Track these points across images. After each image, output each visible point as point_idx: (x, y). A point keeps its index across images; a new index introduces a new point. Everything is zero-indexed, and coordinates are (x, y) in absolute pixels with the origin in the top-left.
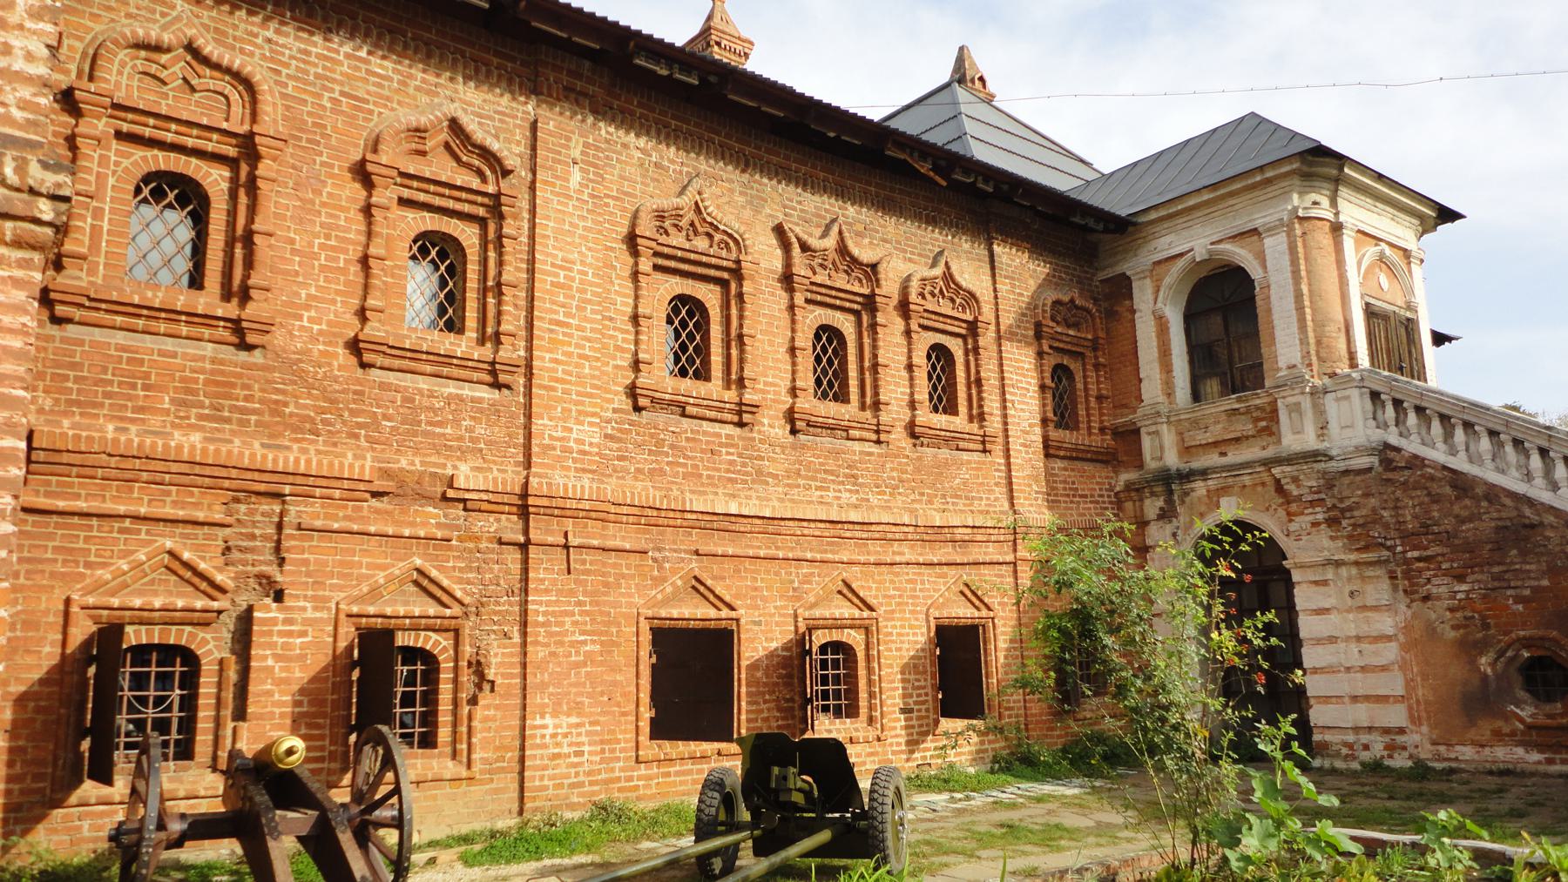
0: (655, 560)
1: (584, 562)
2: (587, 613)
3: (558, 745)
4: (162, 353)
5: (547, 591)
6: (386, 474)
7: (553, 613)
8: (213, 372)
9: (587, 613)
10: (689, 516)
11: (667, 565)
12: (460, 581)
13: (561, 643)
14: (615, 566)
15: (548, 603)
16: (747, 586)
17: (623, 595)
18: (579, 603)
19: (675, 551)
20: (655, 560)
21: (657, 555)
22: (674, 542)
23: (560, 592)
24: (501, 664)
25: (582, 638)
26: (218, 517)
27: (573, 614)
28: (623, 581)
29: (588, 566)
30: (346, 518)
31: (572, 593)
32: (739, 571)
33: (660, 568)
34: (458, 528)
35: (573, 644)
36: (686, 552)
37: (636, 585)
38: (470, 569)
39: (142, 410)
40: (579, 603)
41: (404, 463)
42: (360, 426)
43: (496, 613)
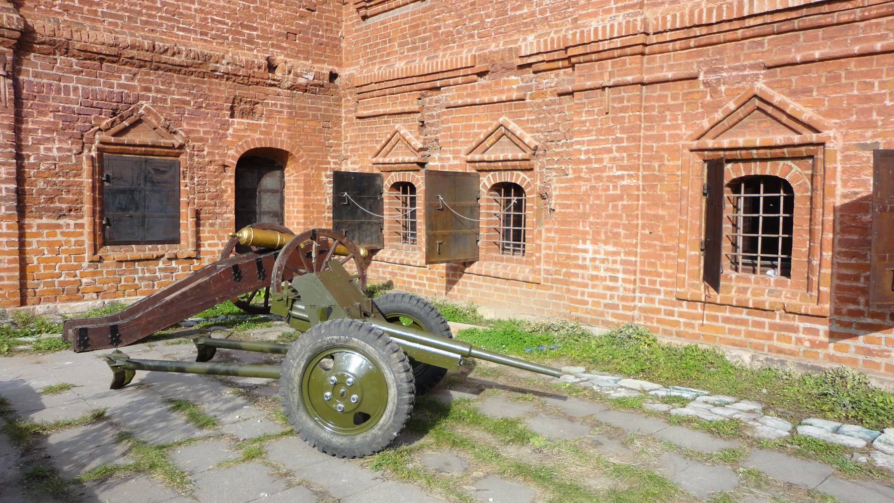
0: (706, 84)
1: (621, 100)
2: (625, 149)
3: (596, 268)
4: (396, 18)
5: (588, 132)
6: (484, 58)
7: (594, 152)
8: (413, 20)
9: (625, 149)
10: (752, 22)
11: (723, 88)
12: (532, 130)
13: (599, 179)
14: (661, 98)
15: (590, 142)
16: (850, 97)
17: (667, 128)
18: (617, 140)
19: (736, 69)
20: (706, 84)
21: (712, 77)
22: (737, 58)
23: (599, 132)
24: (558, 196)
25: (620, 173)
26: (415, 107)
27: (610, 151)
28: (667, 113)
29: (626, 103)
30: (468, 95)
31: (610, 131)
32: (837, 78)
33: (715, 91)
34: (530, 88)
35: (610, 179)
36: (752, 67)
37: (684, 115)
38: (539, 120)
39: (388, 54)
40: (617, 140)
41: (493, 47)
42: (474, 27)
43: (557, 154)
